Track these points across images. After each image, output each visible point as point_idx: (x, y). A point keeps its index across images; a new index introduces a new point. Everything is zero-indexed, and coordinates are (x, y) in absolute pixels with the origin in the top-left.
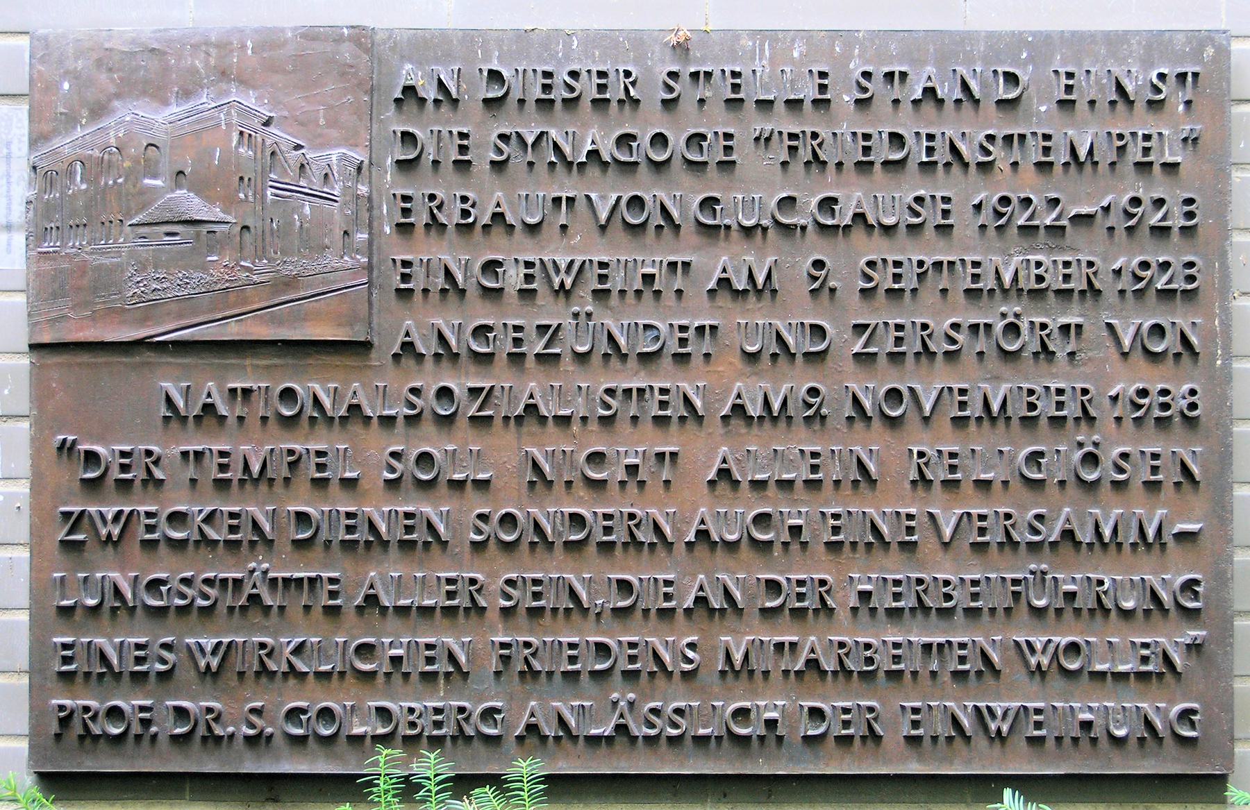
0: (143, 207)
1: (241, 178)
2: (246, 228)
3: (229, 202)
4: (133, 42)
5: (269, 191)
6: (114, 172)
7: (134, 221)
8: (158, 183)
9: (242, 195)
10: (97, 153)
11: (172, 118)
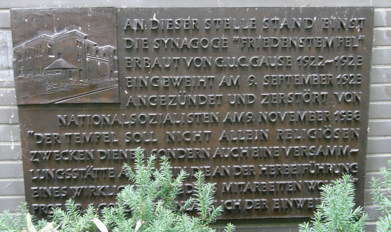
0: (49, 64)
1: (78, 55)
2: (81, 70)
3: (75, 62)
4: (42, 12)
5: (87, 59)
6: (39, 53)
7: (46, 68)
8: (53, 56)
9: (79, 60)
10: (33, 48)
11: (56, 37)
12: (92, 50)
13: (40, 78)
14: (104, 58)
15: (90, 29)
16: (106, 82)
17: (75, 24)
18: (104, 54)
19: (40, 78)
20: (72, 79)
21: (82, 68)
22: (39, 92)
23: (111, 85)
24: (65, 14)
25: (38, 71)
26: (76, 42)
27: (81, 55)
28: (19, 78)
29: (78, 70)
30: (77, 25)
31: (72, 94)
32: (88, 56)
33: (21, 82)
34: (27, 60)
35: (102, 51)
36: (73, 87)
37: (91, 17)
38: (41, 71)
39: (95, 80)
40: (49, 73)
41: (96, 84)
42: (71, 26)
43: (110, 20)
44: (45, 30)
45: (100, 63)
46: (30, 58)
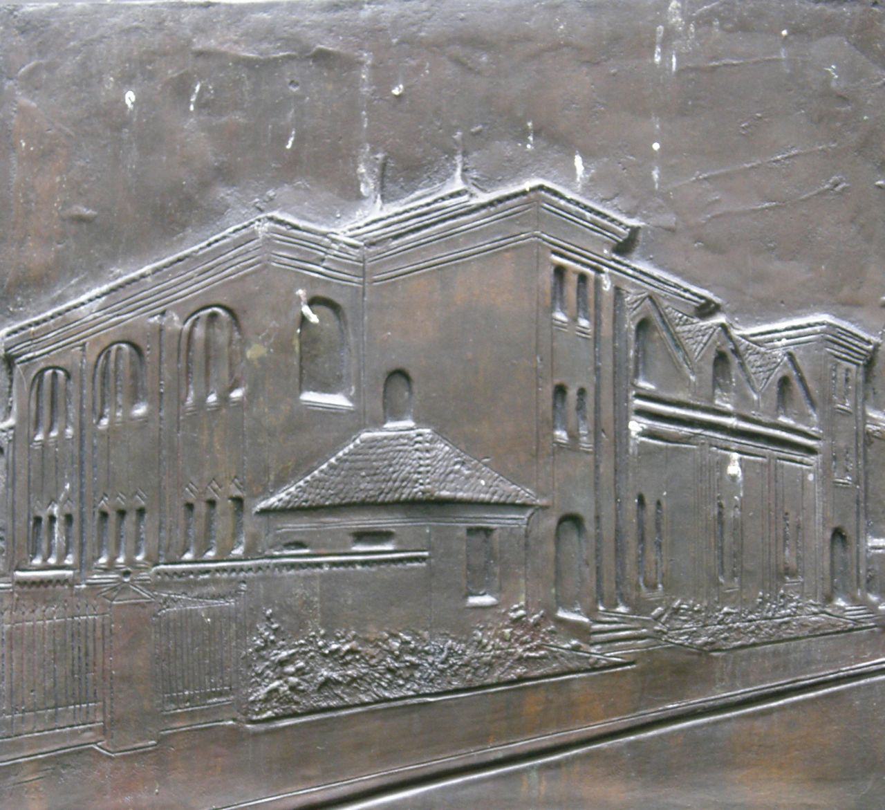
0: (303, 464)
1: (560, 390)
2: (572, 520)
3: (529, 453)
4: (268, 33)
5: (636, 426)
6: (221, 372)
7: (273, 501)
8: (338, 400)
9: (561, 435)
10: (175, 322)
11: (376, 231)
12: (679, 346)
13: (213, 589)
14: (783, 420)
15: (667, 171)
16: (793, 632)
17: (537, 133)
18: (784, 382)
19: (213, 589)
20: (487, 600)
21: (582, 505)
22: (192, 715)
23: (832, 662)
24: (457, 50)
25: (201, 519)
26: (547, 276)
27: (582, 392)
28: (23, 583)
29: (552, 522)
30: (558, 142)
31: (480, 739)
32: (638, 402)
33: (44, 618)
34: (111, 428)
35: (769, 365)
36: (497, 674)
37: (680, 71)
38: (223, 524)
39: (693, 614)
40: (288, 546)
41: (702, 651)
42: (506, 148)
43: (843, 99)
44: (276, 182)
45: (743, 465)
46: (140, 410)
